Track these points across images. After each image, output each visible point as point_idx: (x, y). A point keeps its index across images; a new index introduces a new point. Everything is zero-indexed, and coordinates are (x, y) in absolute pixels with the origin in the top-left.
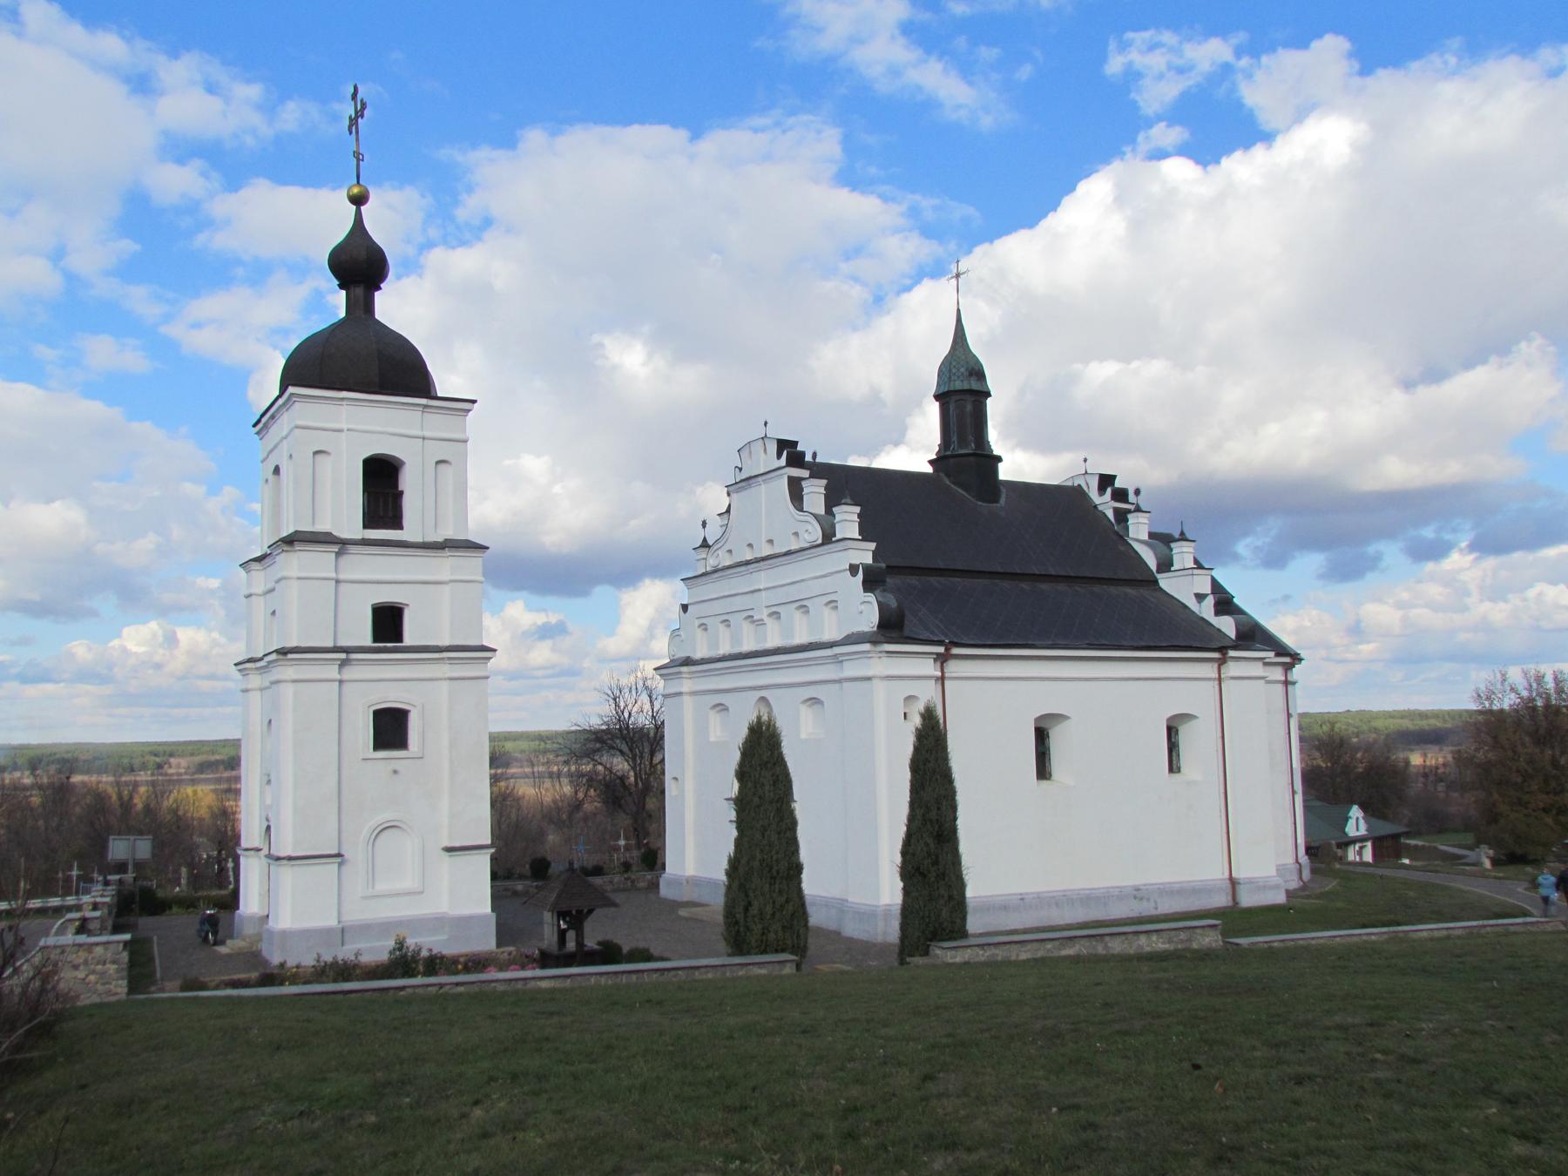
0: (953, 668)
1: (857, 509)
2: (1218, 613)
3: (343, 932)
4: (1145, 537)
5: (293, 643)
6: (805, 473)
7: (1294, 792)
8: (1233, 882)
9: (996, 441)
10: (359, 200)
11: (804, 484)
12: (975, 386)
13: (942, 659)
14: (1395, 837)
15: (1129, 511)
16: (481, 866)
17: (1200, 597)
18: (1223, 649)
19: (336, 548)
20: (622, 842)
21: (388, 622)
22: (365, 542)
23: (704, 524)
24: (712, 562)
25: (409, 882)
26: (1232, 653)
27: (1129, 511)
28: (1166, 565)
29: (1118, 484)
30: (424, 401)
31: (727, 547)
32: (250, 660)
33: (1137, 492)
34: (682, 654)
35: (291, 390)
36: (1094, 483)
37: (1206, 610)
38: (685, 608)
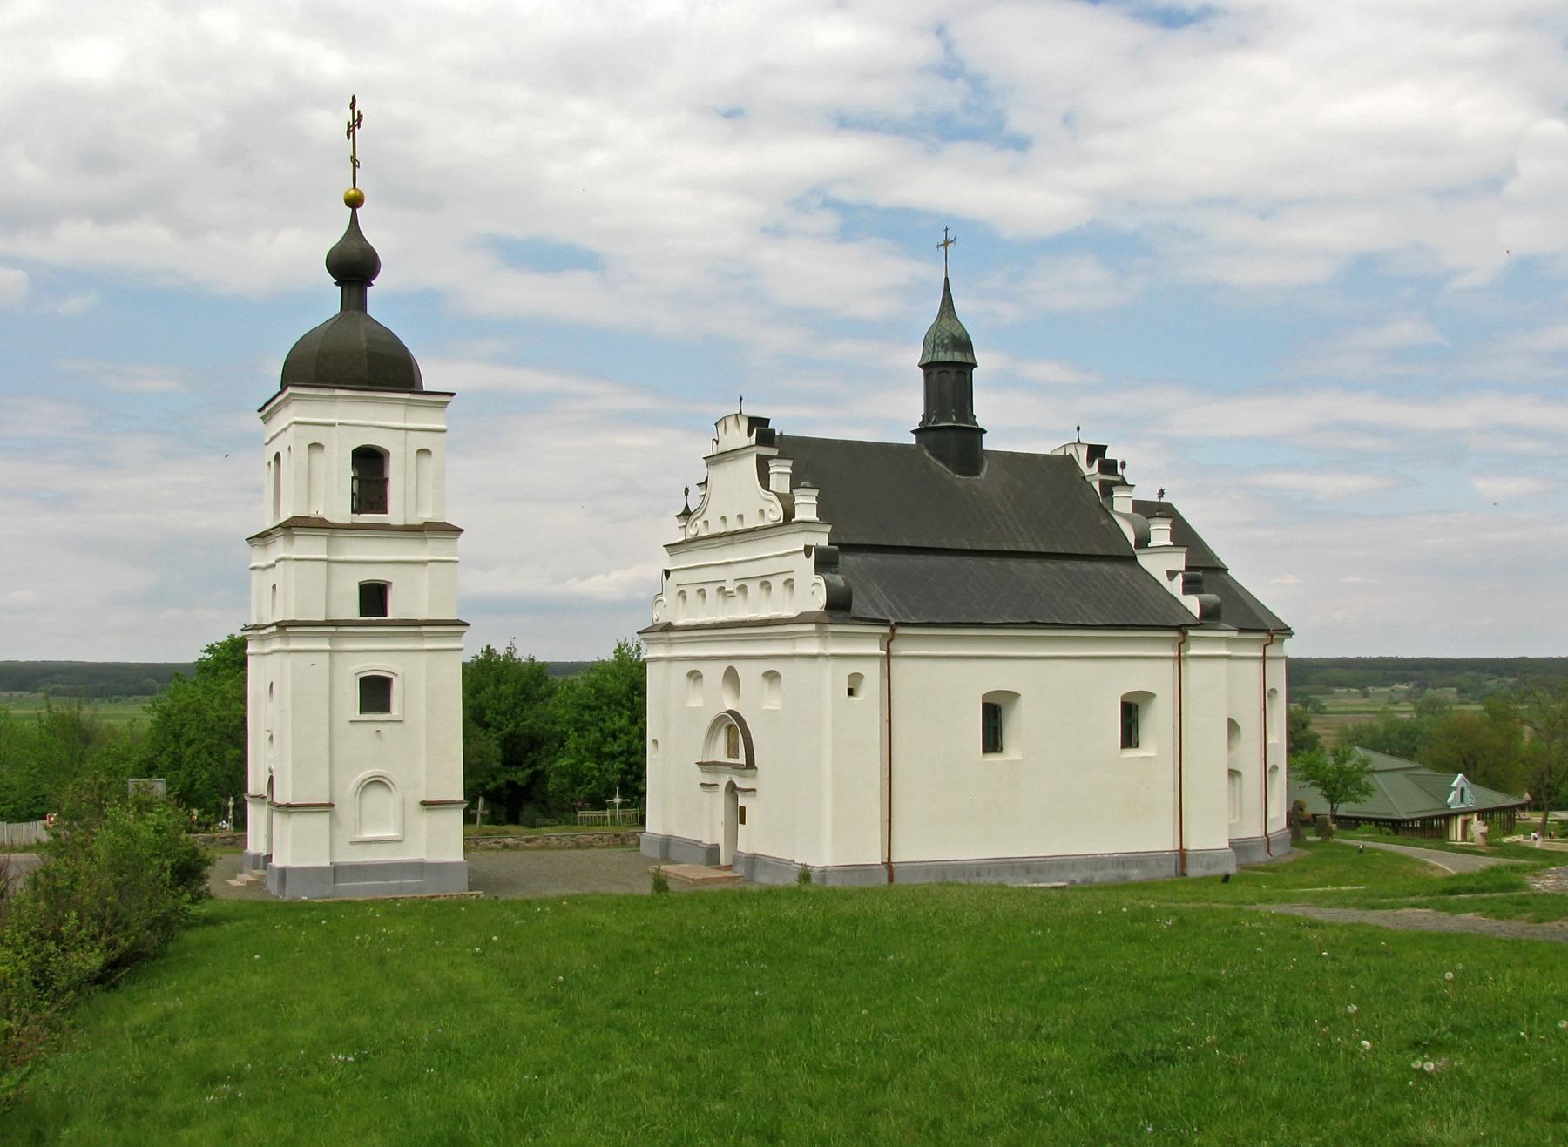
0: (900, 648)
1: (816, 492)
2: (1185, 592)
3: (337, 871)
4: (1129, 510)
6: (774, 452)
7: (1268, 771)
8: (1182, 854)
9: (984, 409)
10: (354, 203)
11: (772, 463)
12: (958, 357)
13: (888, 642)
14: (1512, 808)
15: (1116, 484)
17: (1171, 575)
18: (1182, 629)
20: (617, 800)
21: (374, 597)
23: (687, 492)
24: (692, 532)
25: (390, 833)
26: (1191, 633)
27: (1116, 484)
28: (1143, 541)
30: (407, 396)
31: (704, 518)
32: (255, 628)
33: (1123, 465)
34: (663, 620)
35: (290, 390)
36: (1084, 453)
37: (1175, 587)
38: (667, 573)
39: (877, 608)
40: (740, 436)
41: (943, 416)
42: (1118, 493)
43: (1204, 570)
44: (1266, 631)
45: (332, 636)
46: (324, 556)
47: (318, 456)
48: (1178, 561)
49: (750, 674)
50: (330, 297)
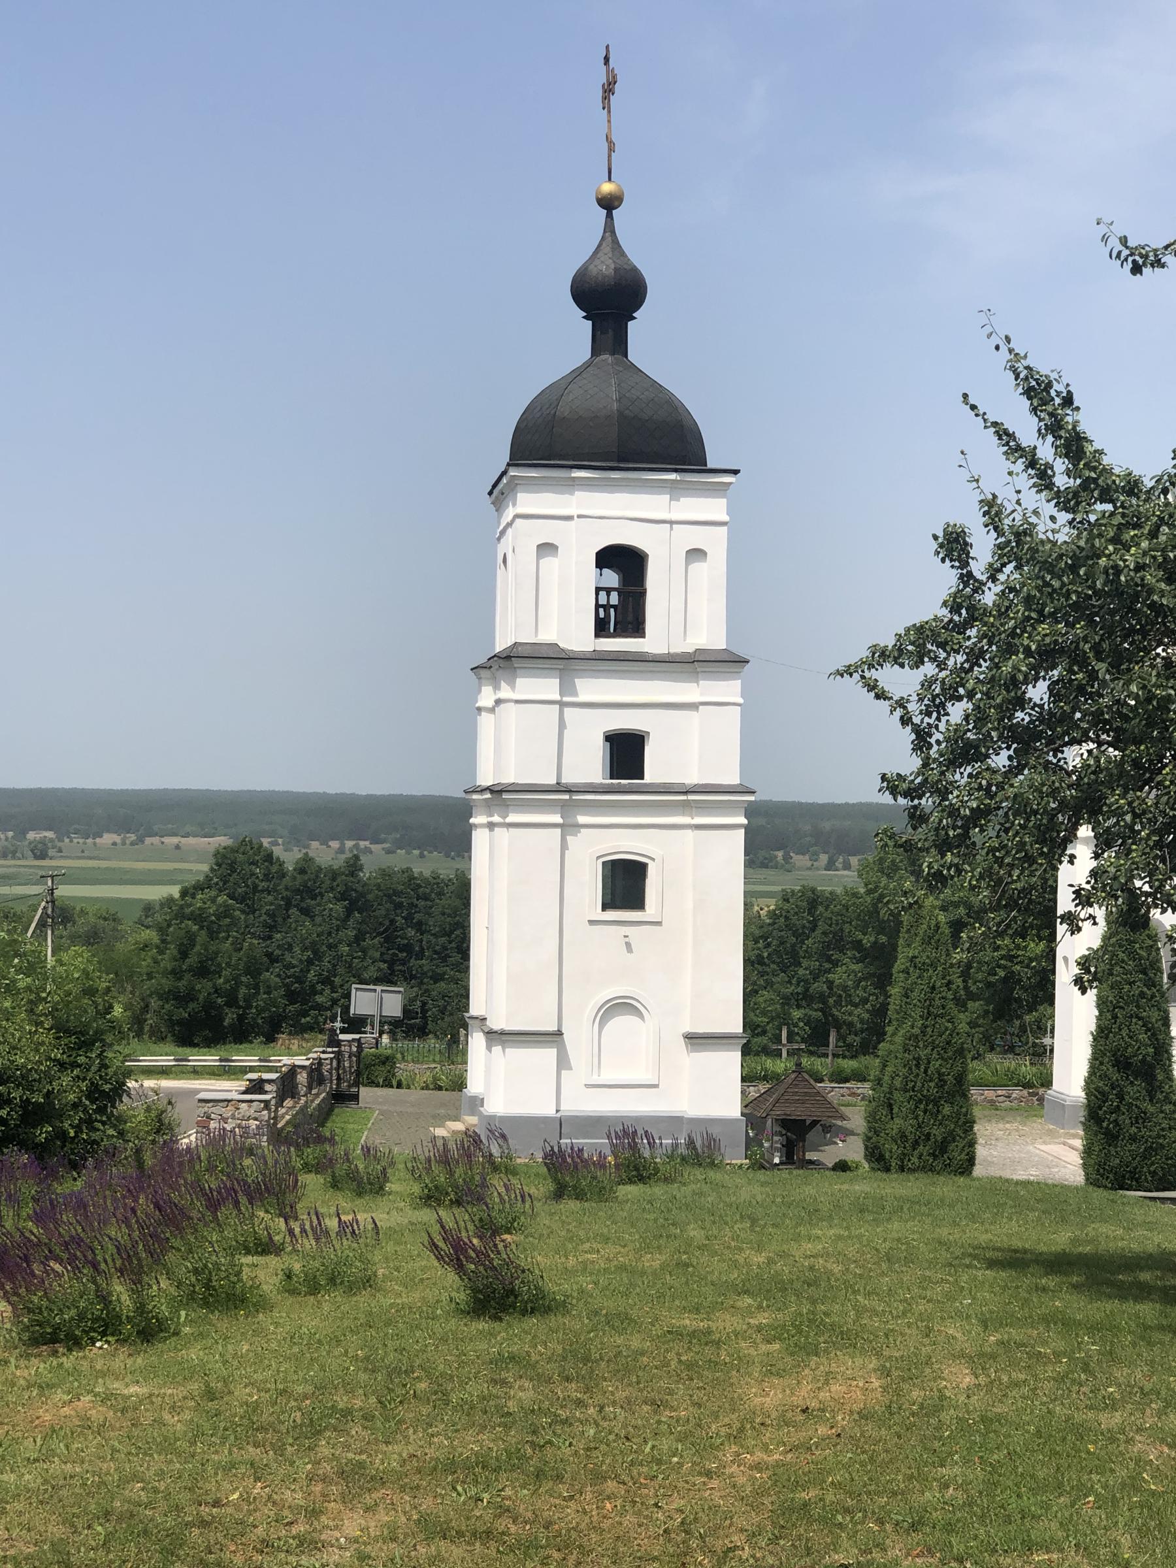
5: (510, 777)
16: (731, 1062)
19: (560, 664)
21: (626, 752)
30: (673, 476)
35: (513, 472)
45: (564, 808)
46: (557, 697)
47: (548, 562)
50: (575, 334)
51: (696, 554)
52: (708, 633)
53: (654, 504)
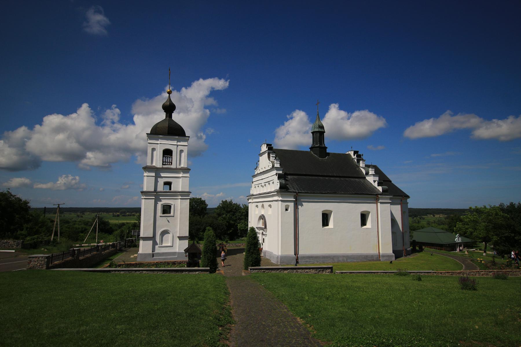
2: (378, 186)
9: (326, 143)
12: (320, 130)
13: (296, 197)
22: (163, 168)
25: (170, 244)
27: (361, 160)
28: (367, 174)
29: (359, 153)
36: (353, 152)
37: (376, 184)
39: (294, 189)
40: (264, 148)
41: (317, 144)
42: (361, 162)
43: (384, 180)
44: (402, 196)
45: (155, 196)
48: (377, 178)
49: (266, 204)
51: (181, 151)
52: (183, 165)
53: (175, 143)
